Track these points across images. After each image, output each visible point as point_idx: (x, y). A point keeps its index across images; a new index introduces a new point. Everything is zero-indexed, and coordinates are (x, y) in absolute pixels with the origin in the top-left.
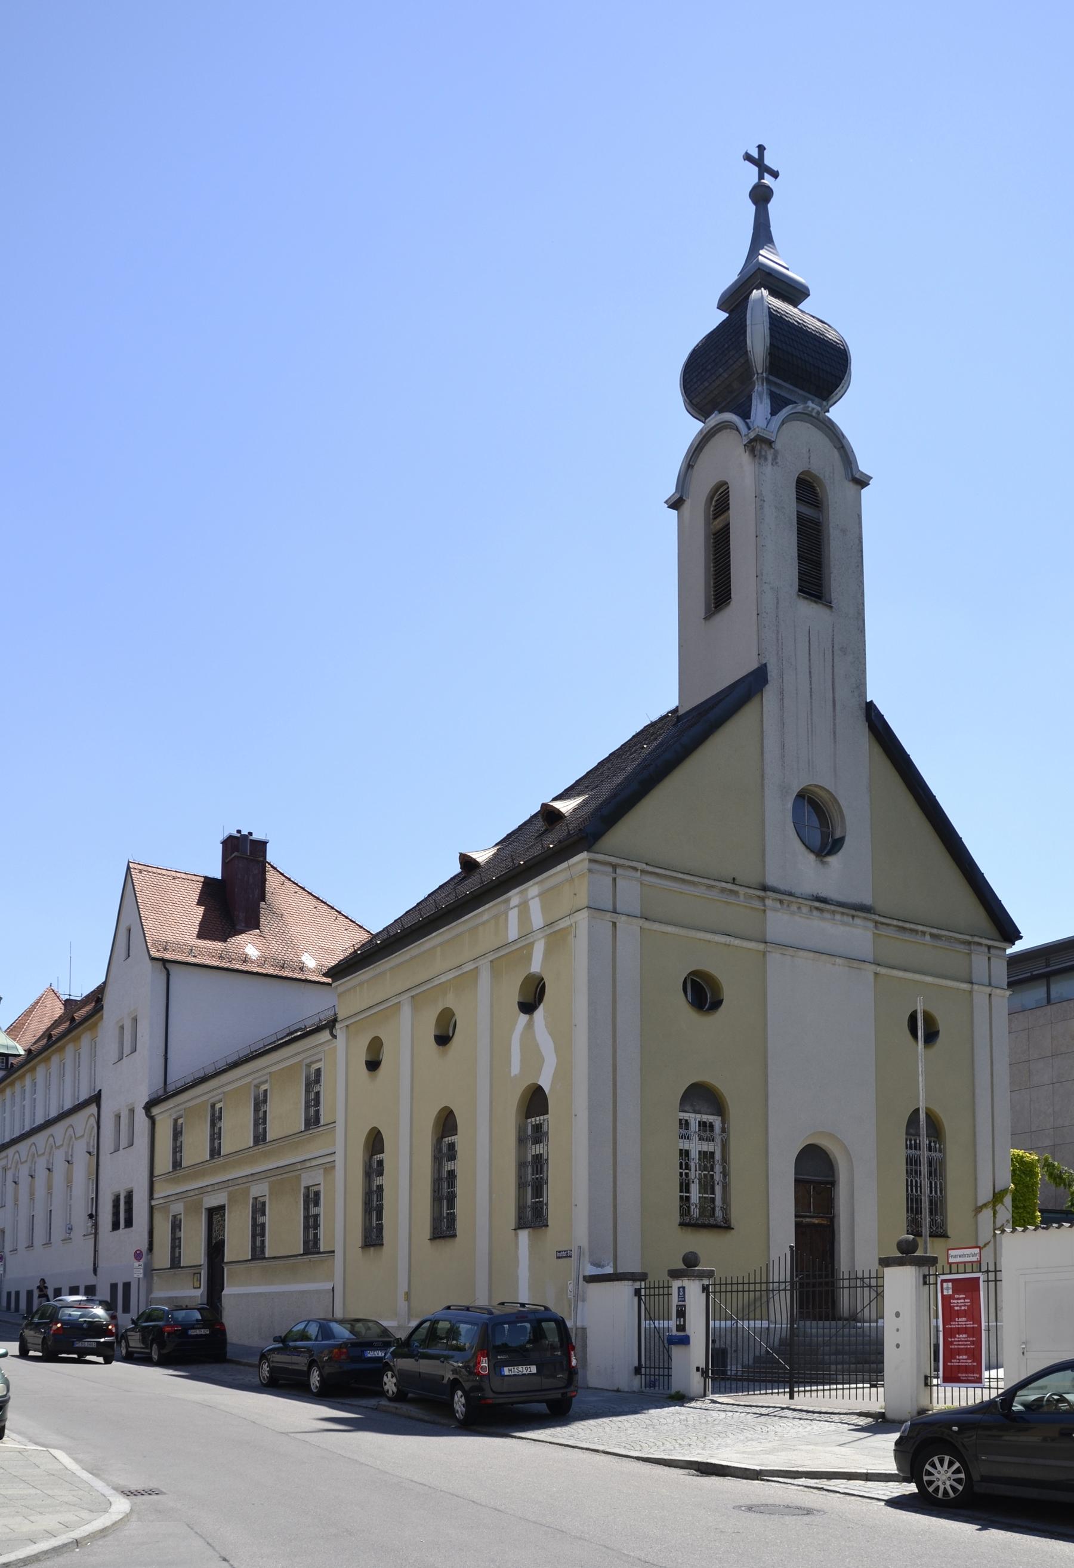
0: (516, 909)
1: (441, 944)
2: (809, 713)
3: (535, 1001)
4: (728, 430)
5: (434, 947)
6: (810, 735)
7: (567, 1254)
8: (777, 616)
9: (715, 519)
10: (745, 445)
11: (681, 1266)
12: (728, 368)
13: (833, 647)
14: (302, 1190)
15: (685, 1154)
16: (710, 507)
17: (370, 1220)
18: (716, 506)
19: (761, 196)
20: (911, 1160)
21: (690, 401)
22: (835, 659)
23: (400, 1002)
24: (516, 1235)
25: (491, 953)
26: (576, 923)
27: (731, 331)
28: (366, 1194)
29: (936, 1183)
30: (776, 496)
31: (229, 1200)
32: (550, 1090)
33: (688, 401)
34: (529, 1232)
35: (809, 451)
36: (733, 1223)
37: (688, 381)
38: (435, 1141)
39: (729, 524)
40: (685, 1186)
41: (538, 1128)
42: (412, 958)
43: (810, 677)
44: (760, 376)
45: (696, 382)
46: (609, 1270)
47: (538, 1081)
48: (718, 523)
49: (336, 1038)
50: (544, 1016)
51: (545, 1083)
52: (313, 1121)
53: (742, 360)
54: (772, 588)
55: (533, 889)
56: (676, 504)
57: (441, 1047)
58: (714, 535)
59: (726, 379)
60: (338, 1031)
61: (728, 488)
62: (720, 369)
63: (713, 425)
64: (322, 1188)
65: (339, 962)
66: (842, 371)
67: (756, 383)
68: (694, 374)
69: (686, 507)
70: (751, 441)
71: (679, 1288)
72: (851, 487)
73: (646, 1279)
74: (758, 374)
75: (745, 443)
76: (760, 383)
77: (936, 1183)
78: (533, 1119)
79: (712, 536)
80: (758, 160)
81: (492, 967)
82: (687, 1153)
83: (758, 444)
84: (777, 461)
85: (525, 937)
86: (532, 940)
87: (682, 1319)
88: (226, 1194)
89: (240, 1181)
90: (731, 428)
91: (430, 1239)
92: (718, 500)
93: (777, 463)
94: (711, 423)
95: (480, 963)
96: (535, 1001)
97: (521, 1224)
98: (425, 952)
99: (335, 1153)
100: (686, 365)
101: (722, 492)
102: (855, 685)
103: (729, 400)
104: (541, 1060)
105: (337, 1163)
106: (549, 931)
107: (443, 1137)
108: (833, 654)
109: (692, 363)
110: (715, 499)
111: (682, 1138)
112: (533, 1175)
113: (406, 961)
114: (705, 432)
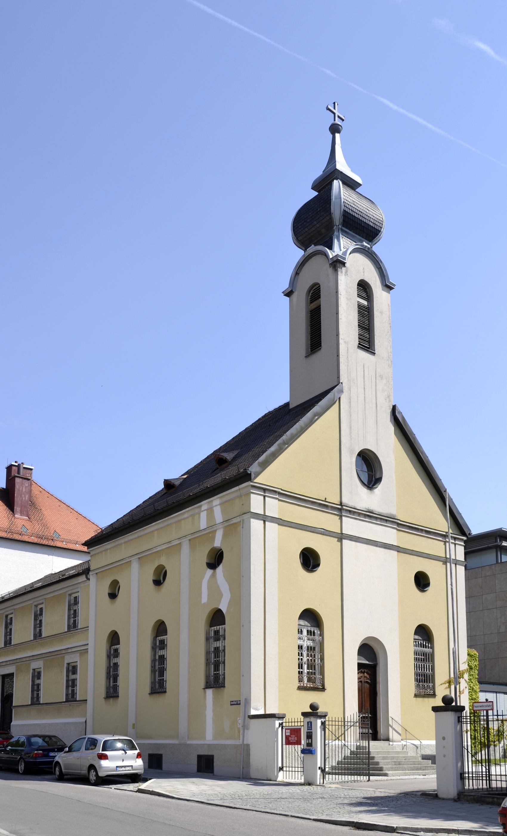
0: (205, 512)
1: (156, 530)
2: (364, 410)
3: (215, 562)
4: (320, 255)
5: (153, 531)
6: (364, 422)
8: (347, 357)
9: (311, 303)
10: (330, 264)
11: (309, 710)
12: (319, 222)
13: (376, 375)
14: (65, 665)
15: (300, 647)
16: (308, 296)
17: (110, 682)
18: (311, 296)
20: (416, 653)
21: (297, 238)
22: (377, 381)
23: (131, 561)
24: (205, 692)
25: (190, 535)
26: (243, 520)
27: (322, 201)
28: (108, 668)
29: (426, 665)
30: (347, 292)
31: (17, 670)
32: (226, 612)
33: (296, 238)
34: (213, 691)
35: (364, 269)
36: (326, 686)
37: (296, 227)
38: (152, 639)
39: (320, 306)
40: (300, 666)
41: (217, 632)
42: (139, 537)
43: (364, 391)
44: (337, 227)
45: (301, 228)
46: (262, 712)
47: (219, 606)
48: (314, 305)
49: (89, 580)
50: (223, 571)
52: (73, 626)
53: (328, 218)
54: (345, 342)
55: (216, 501)
56: (289, 294)
57: (157, 587)
58: (311, 311)
59: (318, 227)
60: (91, 576)
61: (320, 286)
62: (315, 222)
63: (311, 252)
64: (78, 664)
65: (92, 537)
66: (380, 227)
67: (335, 231)
68: (300, 224)
69: (295, 296)
70: (334, 262)
71: (308, 722)
73: (284, 717)
74: (336, 225)
75: (330, 263)
76: (337, 231)
77: (426, 665)
78: (215, 627)
79: (310, 312)
81: (190, 543)
82: (302, 647)
83: (338, 264)
84: (348, 273)
85: (211, 527)
86: (215, 529)
87: (310, 740)
88: (15, 666)
89: (24, 660)
90: (321, 254)
91: (149, 694)
93: (347, 274)
94: (310, 250)
95: (183, 540)
96: (215, 562)
97: (208, 686)
98: (147, 533)
99: (88, 644)
100: (295, 218)
102: (387, 396)
103: (319, 239)
104: (221, 595)
105: (89, 650)
106: (226, 524)
107: (157, 636)
108: (376, 379)
109: (307, 218)
110: (311, 292)
111: (299, 639)
112: (215, 658)
113: (135, 538)
114: (306, 256)
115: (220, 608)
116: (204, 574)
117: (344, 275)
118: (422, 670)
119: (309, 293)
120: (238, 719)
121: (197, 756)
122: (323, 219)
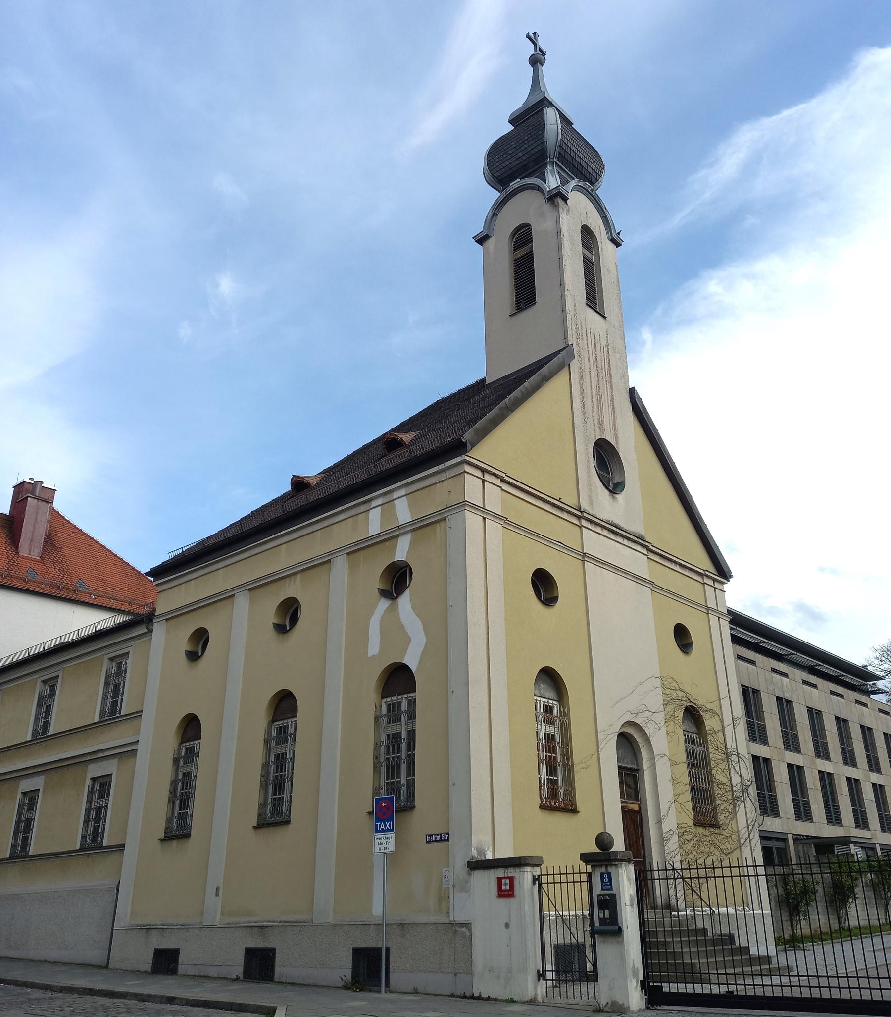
7: (441, 837)
19: (536, 61)
27: (530, 128)
32: (417, 669)
37: (491, 161)
46: (489, 856)
48: (522, 251)
51: (412, 661)
56: (481, 240)
57: (281, 636)
62: (520, 153)
69: (490, 243)
72: (611, 246)
80: (532, 38)
90: (531, 189)
92: (517, 238)
101: (522, 233)
115: (406, 661)
116: (374, 607)
117: (565, 213)
118: (697, 783)
119: (514, 236)
120: (444, 870)
121: (351, 951)
122: (533, 149)
